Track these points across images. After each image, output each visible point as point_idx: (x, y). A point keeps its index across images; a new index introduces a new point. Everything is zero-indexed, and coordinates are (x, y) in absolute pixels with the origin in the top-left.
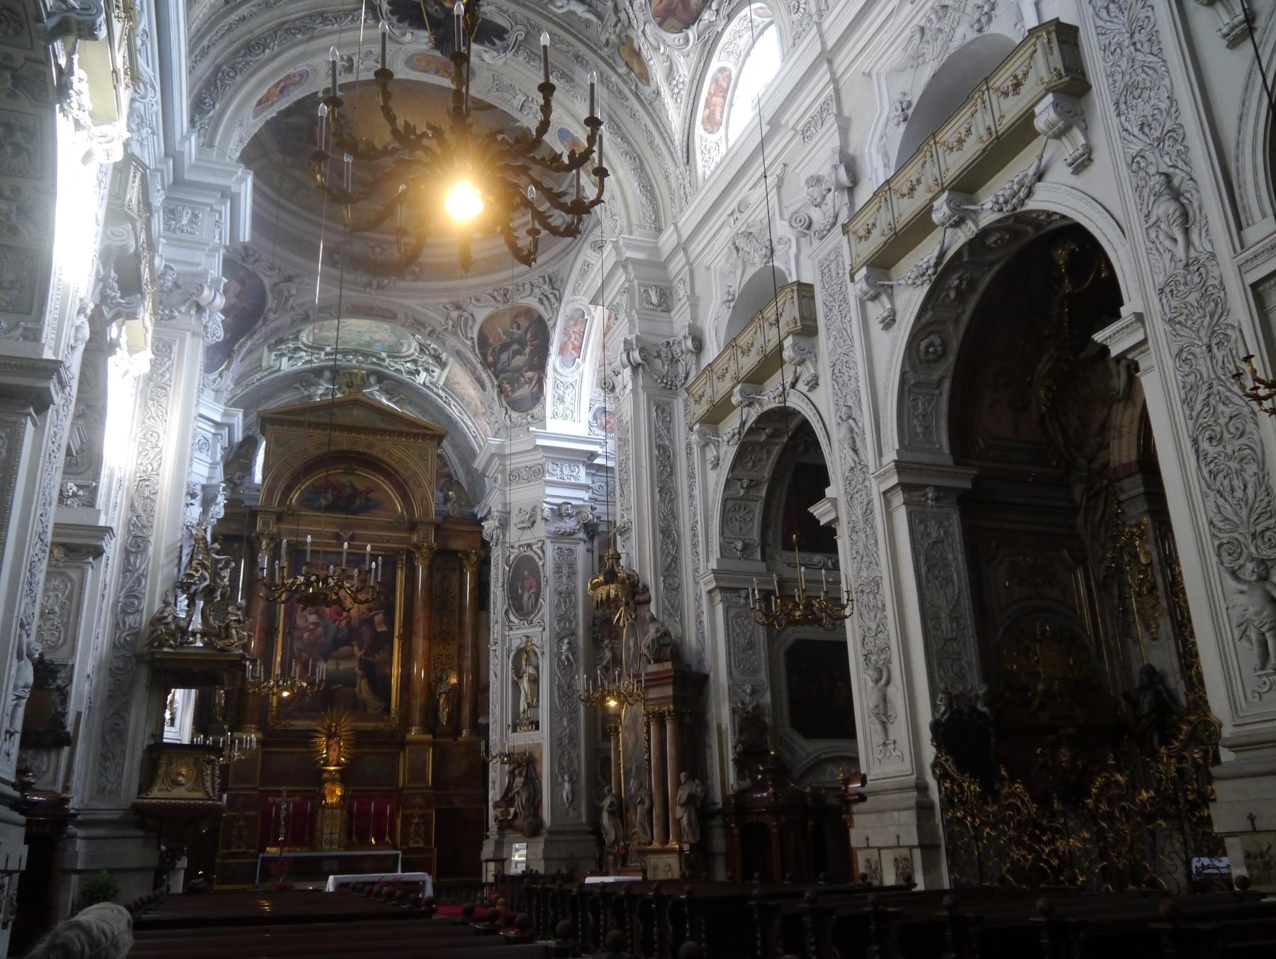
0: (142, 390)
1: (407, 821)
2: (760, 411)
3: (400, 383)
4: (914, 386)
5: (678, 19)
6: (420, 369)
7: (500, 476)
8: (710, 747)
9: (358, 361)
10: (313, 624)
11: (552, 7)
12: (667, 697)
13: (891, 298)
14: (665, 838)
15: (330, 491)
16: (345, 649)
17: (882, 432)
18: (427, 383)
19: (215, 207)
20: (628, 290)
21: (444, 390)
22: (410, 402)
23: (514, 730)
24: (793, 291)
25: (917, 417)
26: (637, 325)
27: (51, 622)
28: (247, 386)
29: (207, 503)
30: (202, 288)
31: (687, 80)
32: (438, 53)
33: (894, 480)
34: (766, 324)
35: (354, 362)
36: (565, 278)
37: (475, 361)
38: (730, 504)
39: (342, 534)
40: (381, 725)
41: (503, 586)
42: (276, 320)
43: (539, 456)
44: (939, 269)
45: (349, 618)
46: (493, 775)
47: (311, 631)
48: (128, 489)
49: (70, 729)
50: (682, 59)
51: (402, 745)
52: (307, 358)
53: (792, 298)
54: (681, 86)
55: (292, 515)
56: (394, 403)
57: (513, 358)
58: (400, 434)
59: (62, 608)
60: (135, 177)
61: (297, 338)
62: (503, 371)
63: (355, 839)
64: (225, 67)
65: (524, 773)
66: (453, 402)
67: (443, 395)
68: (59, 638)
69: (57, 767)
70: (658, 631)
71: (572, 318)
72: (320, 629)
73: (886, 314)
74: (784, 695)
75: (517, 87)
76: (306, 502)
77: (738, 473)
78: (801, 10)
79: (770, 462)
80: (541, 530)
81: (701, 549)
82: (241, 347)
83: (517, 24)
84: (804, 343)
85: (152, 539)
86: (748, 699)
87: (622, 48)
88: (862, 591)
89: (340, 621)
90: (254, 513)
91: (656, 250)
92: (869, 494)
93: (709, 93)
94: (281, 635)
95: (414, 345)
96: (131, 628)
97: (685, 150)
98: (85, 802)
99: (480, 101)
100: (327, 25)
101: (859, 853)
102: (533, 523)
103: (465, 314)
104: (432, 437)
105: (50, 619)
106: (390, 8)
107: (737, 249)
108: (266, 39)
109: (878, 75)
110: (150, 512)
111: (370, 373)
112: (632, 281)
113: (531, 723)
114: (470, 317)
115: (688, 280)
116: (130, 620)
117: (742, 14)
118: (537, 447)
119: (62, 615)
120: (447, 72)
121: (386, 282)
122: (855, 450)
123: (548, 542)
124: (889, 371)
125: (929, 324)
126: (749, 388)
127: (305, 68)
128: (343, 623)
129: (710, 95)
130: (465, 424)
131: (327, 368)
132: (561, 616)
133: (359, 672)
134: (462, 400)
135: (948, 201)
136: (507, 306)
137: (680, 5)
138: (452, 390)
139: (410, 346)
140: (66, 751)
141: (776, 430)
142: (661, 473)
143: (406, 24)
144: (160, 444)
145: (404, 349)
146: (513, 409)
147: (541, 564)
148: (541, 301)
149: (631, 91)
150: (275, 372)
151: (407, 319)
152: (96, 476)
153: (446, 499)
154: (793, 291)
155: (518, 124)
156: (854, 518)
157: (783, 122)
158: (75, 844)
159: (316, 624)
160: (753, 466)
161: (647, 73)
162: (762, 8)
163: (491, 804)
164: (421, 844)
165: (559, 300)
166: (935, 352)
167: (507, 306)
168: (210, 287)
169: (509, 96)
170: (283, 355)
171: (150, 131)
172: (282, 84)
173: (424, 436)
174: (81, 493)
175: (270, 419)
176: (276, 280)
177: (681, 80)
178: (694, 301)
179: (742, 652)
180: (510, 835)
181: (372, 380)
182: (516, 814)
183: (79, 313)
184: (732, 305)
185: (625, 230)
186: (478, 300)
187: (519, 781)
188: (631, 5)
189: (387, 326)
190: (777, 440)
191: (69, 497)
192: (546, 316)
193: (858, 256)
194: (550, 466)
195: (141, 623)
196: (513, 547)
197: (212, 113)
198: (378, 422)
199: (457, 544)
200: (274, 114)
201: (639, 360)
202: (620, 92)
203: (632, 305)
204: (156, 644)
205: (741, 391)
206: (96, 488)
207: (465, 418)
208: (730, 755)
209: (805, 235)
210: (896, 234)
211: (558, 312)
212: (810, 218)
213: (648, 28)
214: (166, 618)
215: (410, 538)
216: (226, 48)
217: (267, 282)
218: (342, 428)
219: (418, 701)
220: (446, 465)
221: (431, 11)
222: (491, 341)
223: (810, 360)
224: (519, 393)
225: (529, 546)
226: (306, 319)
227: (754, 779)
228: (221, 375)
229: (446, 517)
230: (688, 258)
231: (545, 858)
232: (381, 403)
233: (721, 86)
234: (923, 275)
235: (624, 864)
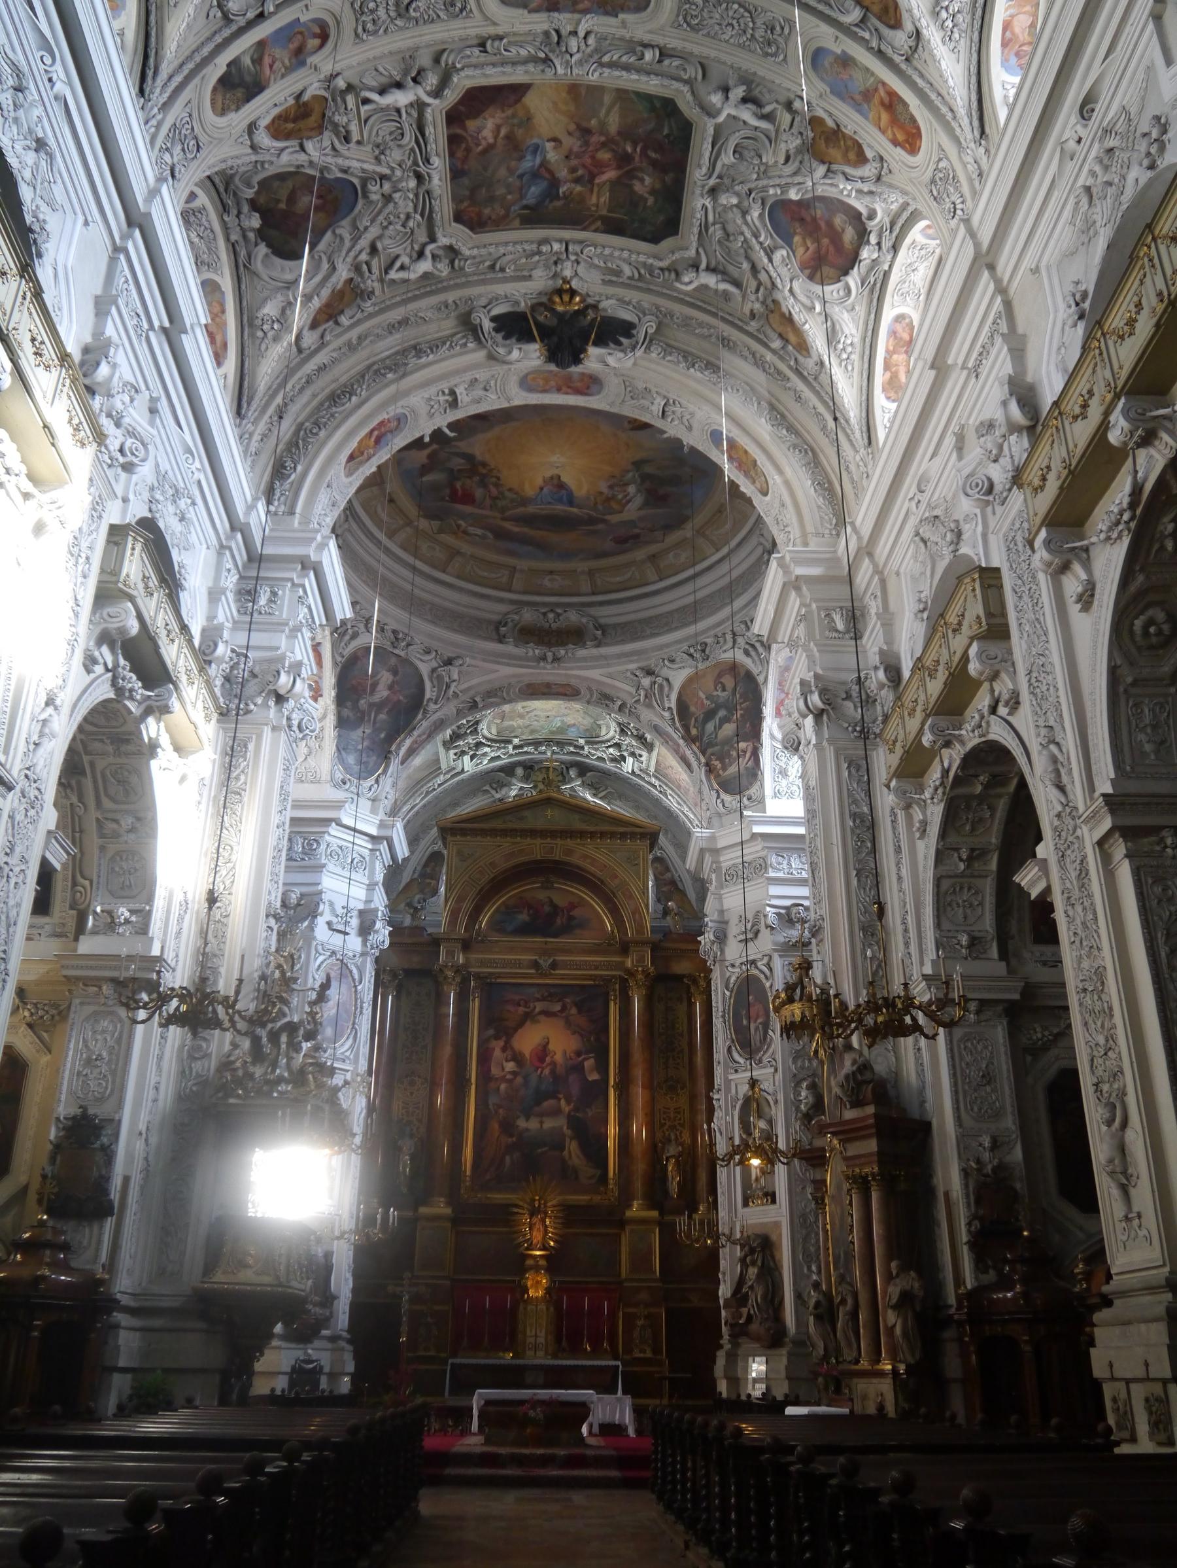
0: (215, 796)
1: (629, 1320)
2: (963, 752)
3: (606, 773)
4: (1135, 683)
5: (833, 266)
6: (625, 754)
7: (714, 876)
8: (939, 1226)
9: (553, 753)
10: (509, 1072)
11: (678, 285)
12: (871, 1154)
13: (1087, 565)
14: (876, 1358)
15: (526, 911)
16: (548, 1104)
17: (1092, 756)
18: (636, 770)
19: (296, 581)
20: (803, 618)
21: (656, 778)
22: (621, 796)
23: (745, 1204)
24: (974, 580)
25: (1143, 730)
26: (818, 662)
27: (98, 1070)
28: (428, 793)
29: (365, 930)
30: (278, 672)
31: (857, 340)
32: (552, 367)
33: (1107, 824)
34: (950, 631)
35: (549, 754)
37: (675, 736)
38: (946, 884)
39: (541, 962)
40: (597, 1199)
41: (723, 1016)
42: (436, 712)
43: (759, 847)
44: (1138, 512)
45: (553, 1064)
46: (724, 1264)
47: (510, 1081)
48: (197, 913)
49: (115, 1195)
50: (846, 315)
51: (622, 1224)
52: (493, 755)
53: (974, 590)
54: (849, 349)
55: (482, 941)
56: (601, 798)
57: (720, 727)
58: (603, 835)
59: (110, 1054)
60: (133, 549)
61: (475, 731)
62: (711, 744)
63: (564, 1343)
64: (307, 424)
65: (759, 1263)
66: (669, 791)
67: (657, 783)
68: (106, 1088)
69: (99, 1242)
70: (854, 1062)
72: (519, 1080)
73: (1080, 589)
74: (1048, 1152)
75: (654, 390)
76: (497, 926)
77: (953, 839)
78: (959, 212)
79: (997, 821)
80: (765, 943)
81: (913, 949)
82: (399, 748)
83: (645, 315)
84: (994, 649)
85: (223, 970)
86: (986, 1156)
87: (771, 316)
88: (1085, 990)
89: (543, 1069)
90: (436, 942)
91: (838, 560)
92: (1082, 848)
93: (887, 351)
94: (473, 1087)
95: (614, 727)
96: (198, 1075)
97: (864, 429)
98: (144, 1284)
99: (636, 420)
100: (420, 358)
101: (1105, 1386)
102: (757, 933)
103: (659, 680)
104: (643, 836)
105: (97, 1067)
106: (492, 325)
107: (924, 541)
108: (352, 385)
109: (1048, 268)
110: (221, 938)
111: (570, 765)
112: (809, 605)
113: (766, 1195)
114: (665, 683)
115: (879, 594)
116: (197, 1066)
117: (908, 241)
118: (754, 836)
119: (110, 1061)
120: (569, 387)
121: (563, 652)
122: (1061, 788)
123: (776, 956)
124: (1094, 670)
125: (1141, 593)
126: (943, 722)
127: (400, 411)
128: (547, 1071)
129: (889, 353)
130: (687, 817)
131: (519, 763)
132: (797, 1052)
133: (568, 1132)
134: (679, 787)
135: (1126, 413)
136: (707, 664)
137: (831, 249)
138: (665, 776)
139: (608, 727)
140: (109, 1223)
141: (994, 776)
142: (858, 851)
143: (514, 340)
144: (234, 858)
145: (603, 732)
146: (726, 791)
147: (768, 985)
148: (747, 653)
149: (790, 367)
150: (458, 774)
151: (592, 696)
152: (150, 899)
153: (666, 912)
154: (974, 580)
155: (666, 436)
156: (1068, 885)
157: (950, 362)
158: (117, 1336)
159: (514, 1073)
160: (973, 829)
161: (805, 341)
162: (928, 227)
163: (721, 1302)
164: (649, 1354)
166: (1160, 632)
167: (707, 664)
168: (288, 672)
169: (646, 403)
170: (463, 753)
171: (189, 501)
172: (376, 433)
173: (633, 836)
174: (133, 919)
175: (452, 829)
176: (434, 664)
177: (849, 342)
178: (888, 621)
179: (975, 1090)
180: (746, 1345)
181: (573, 773)
182: (750, 1318)
183: (47, 704)
184: (925, 615)
185: (798, 541)
186: (672, 661)
187: (752, 1272)
188: (771, 260)
189: (577, 706)
190: (999, 790)
191: (121, 924)
192: (755, 670)
193: (1036, 514)
194: (773, 859)
195: (209, 1070)
196: (733, 966)
197: (293, 477)
198: (577, 824)
199: (682, 967)
200: (374, 469)
201: (820, 705)
202: (779, 372)
203: (810, 635)
204: (220, 1095)
205: (932, 728)
206: (149, 913)
207: (686, 809)
208: (964, 1236)
209: (988, 503)
210: (1070, 472)
212: (989, 479)
213: (796, 285)
214: (233, 1062)
215: (623, 963)
216: (308, 403)
217: (425, 669)
218: (533, 833)
219: (640, 1167)
220: (668, 869)
221: (541, 319)
222: (692, 709)
223: (1007, 672)
224: (732, 770)
225: (753, 962)
226: (474, 706)
227: (1000, 1272)
228: (377, 781)
229: (667, 933)
230: (875, 565)
231: (789, 1378)
232: (585, 799)
233: (901, 339)
234: (1118, 523)
235: (838, 1390)
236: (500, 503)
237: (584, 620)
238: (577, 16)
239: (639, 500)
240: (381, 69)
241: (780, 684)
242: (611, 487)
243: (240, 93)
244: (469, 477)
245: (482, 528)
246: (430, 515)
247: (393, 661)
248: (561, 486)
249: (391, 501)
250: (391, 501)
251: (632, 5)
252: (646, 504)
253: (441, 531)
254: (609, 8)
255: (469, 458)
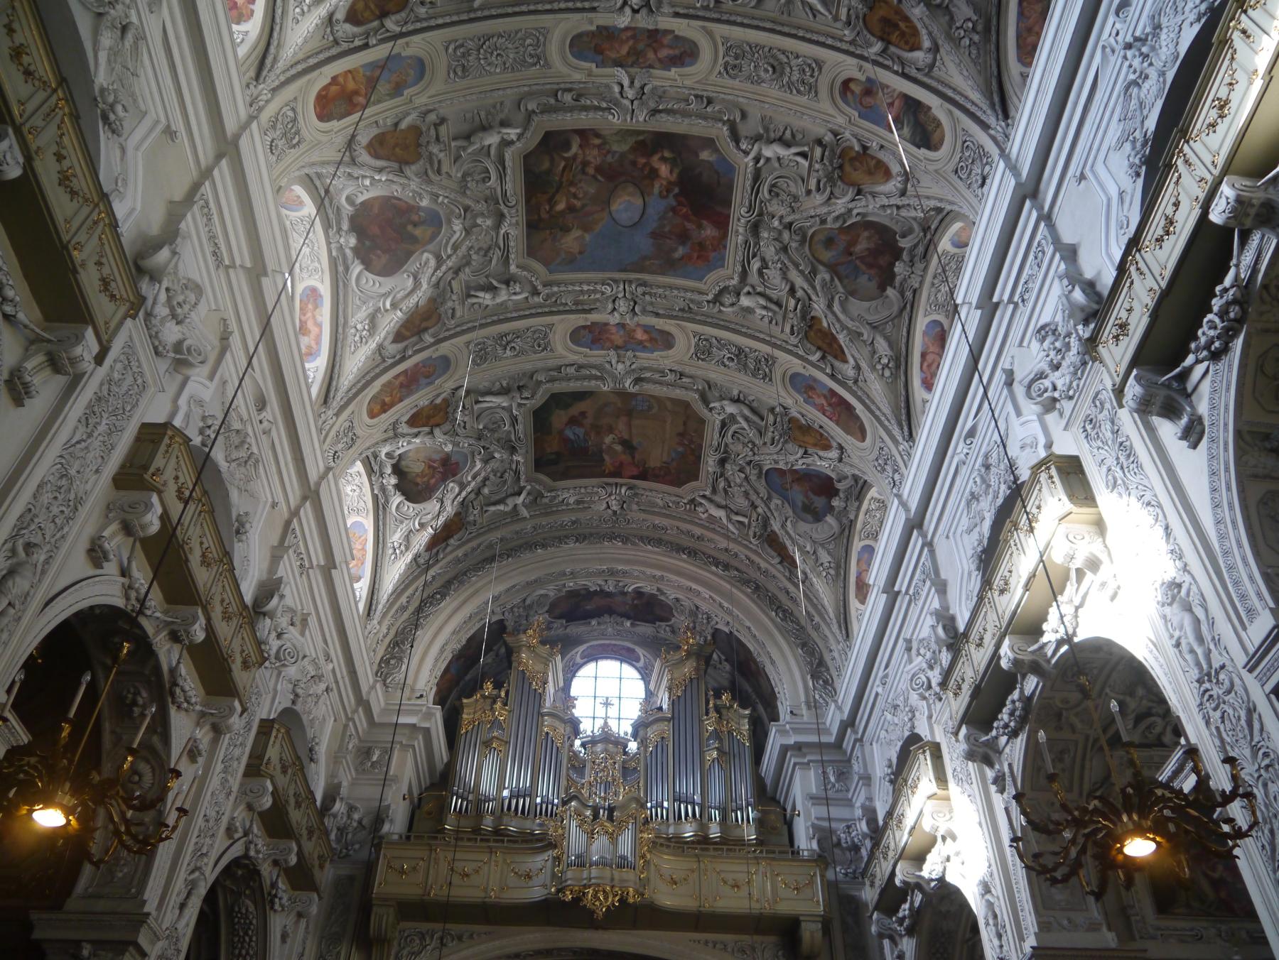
238: (633, 25)
240: (811, 15)
243: (922, 117)
251: (585, 39)
254: (605, 33)
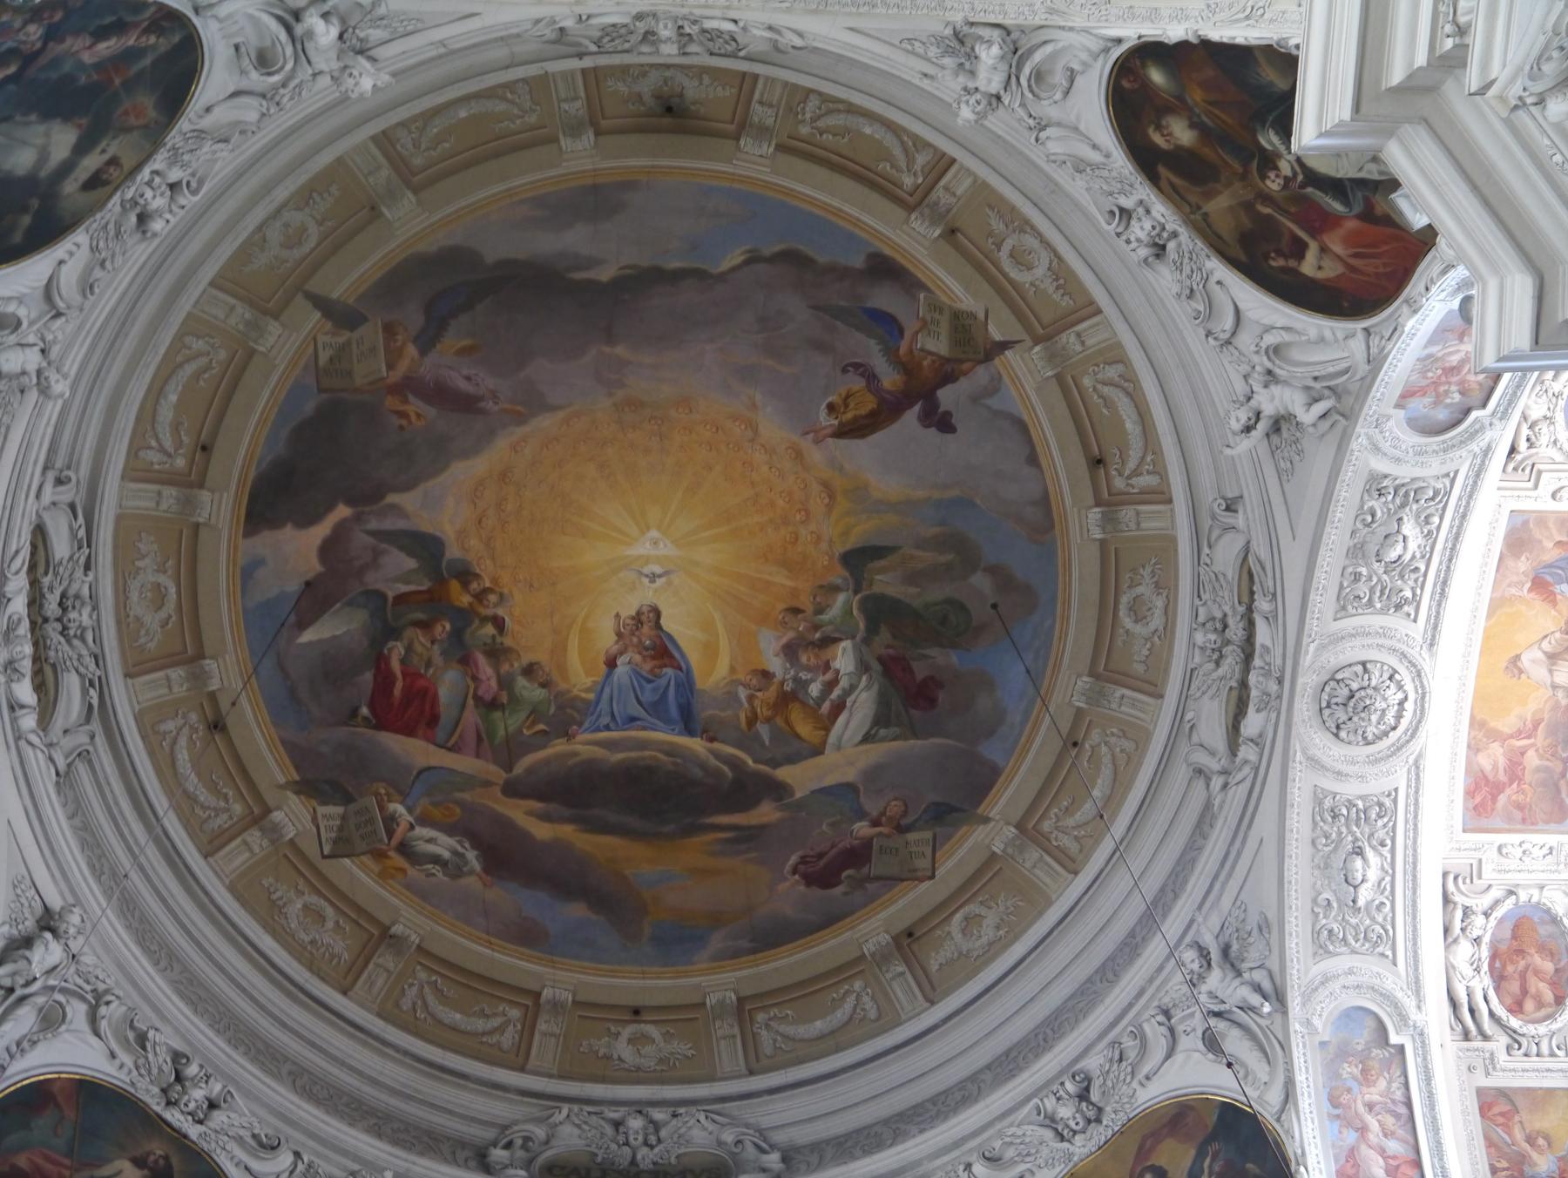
36: (1272, 915)
71: (1343, 1053)
165: (1279, 998)
167: (1100, 1134)
211: (1285, 1047)
236: (507, 724)
237: (728, 1137)
239: (863, 705)
241: (1334, 1102)
242: (790, 651)
244: (425, 626)
245: (450, 830)
246: (310, 787)
247: (157, 1149)
248: (663, 651)
249: (217, 725)
250: (217, 725)
252: (882, 718)
253: (343, 847)
255: (426, 547)
